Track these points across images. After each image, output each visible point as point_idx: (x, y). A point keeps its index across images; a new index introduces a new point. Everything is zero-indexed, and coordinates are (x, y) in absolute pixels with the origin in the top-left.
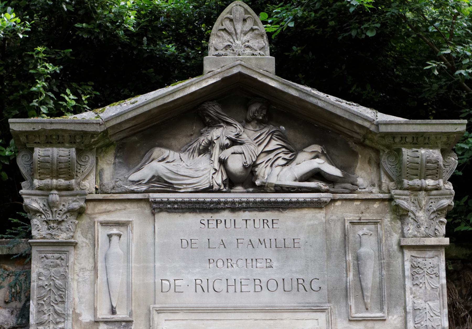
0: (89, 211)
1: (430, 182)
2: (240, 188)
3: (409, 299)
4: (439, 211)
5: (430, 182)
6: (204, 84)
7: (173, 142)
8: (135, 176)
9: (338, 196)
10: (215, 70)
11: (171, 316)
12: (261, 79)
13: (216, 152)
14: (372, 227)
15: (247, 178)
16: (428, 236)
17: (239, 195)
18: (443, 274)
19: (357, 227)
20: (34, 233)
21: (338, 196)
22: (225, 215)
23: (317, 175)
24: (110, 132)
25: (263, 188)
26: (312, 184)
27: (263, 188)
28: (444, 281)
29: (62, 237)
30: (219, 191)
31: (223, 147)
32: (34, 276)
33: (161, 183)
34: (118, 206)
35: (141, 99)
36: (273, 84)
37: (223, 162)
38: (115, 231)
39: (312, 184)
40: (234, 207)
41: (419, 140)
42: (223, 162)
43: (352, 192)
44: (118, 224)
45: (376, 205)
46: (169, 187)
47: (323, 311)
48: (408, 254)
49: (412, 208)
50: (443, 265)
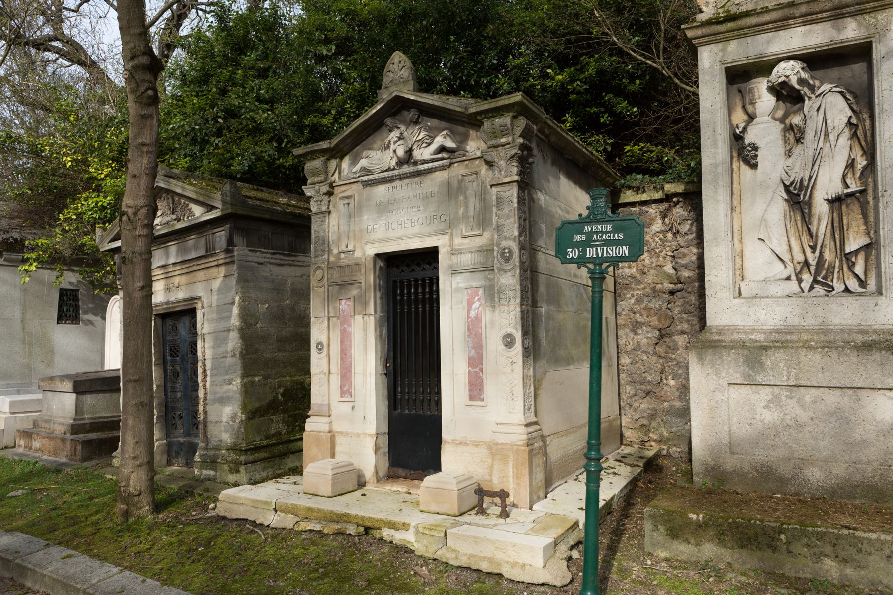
0: (336, 193)
1: (503, 140)
2: (406, 166)
3: (494, 219)
4: (512, 157)
5: (503, 140)
6: (379, 107)
7: (375, 146)
8: (354, 170)
9: (454, 160)
10: (385, 96)
11: (372, 246)
12: (406, 96)
13: (392, 147)
14: (474, 176)
15: (408, 158)
16: (506, 176)
17: (406, 169)
18: (515, 200)
19: (466, 178)
20: (311, 208)
21: (454, 160)
22: (397, 183)
23: (442, 149)
24: (341, 146)
25: (415, 163)
26: (439, 156)
27: (415, 163)
28: (516, 205)
29: (324, 208)
30: (394, 169)
31: (395, 143)
32: (312, 232)
33: (367, 171)
34: (348, 187)
35: (358, 123)
36: (412, 98)
37: (395, 151)
38: (346, 201)
39: (439, 156)
40: (401, 178)
41: (498, 111)
42: (395, 151)
43: (464, 155)
44: (349, 197)
45: (477, 162)
46: (370, 172)
47: (447, 233)
48: (493, 188)
49: (496, 159)
50: (515, 195)
